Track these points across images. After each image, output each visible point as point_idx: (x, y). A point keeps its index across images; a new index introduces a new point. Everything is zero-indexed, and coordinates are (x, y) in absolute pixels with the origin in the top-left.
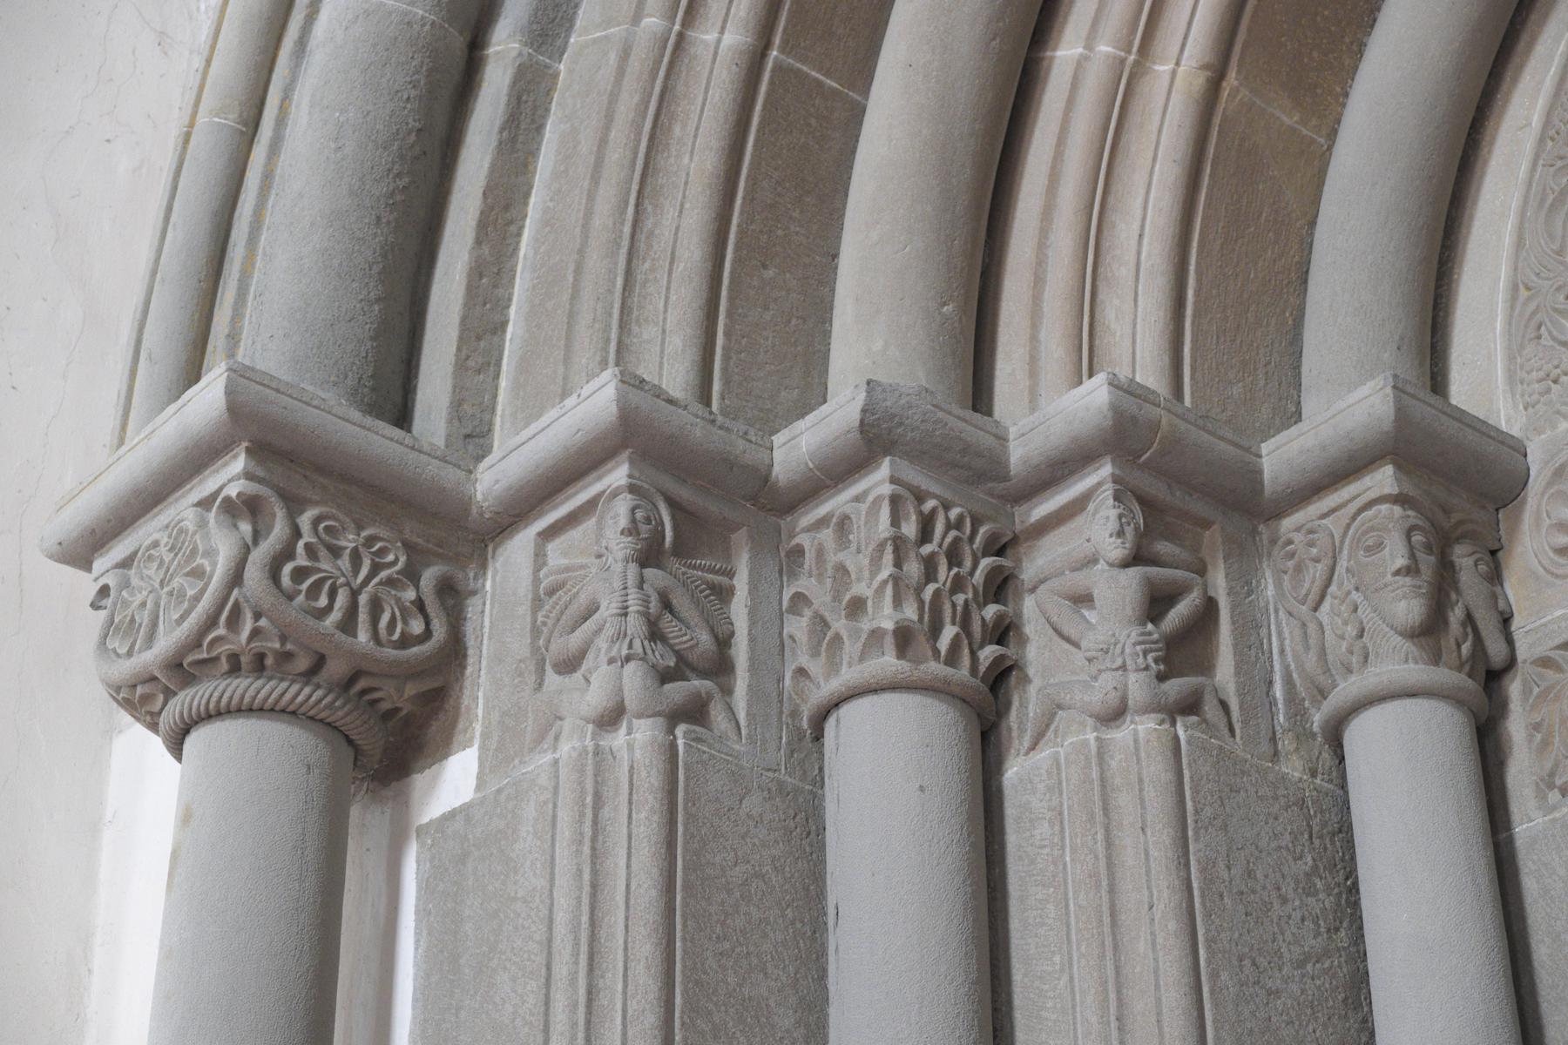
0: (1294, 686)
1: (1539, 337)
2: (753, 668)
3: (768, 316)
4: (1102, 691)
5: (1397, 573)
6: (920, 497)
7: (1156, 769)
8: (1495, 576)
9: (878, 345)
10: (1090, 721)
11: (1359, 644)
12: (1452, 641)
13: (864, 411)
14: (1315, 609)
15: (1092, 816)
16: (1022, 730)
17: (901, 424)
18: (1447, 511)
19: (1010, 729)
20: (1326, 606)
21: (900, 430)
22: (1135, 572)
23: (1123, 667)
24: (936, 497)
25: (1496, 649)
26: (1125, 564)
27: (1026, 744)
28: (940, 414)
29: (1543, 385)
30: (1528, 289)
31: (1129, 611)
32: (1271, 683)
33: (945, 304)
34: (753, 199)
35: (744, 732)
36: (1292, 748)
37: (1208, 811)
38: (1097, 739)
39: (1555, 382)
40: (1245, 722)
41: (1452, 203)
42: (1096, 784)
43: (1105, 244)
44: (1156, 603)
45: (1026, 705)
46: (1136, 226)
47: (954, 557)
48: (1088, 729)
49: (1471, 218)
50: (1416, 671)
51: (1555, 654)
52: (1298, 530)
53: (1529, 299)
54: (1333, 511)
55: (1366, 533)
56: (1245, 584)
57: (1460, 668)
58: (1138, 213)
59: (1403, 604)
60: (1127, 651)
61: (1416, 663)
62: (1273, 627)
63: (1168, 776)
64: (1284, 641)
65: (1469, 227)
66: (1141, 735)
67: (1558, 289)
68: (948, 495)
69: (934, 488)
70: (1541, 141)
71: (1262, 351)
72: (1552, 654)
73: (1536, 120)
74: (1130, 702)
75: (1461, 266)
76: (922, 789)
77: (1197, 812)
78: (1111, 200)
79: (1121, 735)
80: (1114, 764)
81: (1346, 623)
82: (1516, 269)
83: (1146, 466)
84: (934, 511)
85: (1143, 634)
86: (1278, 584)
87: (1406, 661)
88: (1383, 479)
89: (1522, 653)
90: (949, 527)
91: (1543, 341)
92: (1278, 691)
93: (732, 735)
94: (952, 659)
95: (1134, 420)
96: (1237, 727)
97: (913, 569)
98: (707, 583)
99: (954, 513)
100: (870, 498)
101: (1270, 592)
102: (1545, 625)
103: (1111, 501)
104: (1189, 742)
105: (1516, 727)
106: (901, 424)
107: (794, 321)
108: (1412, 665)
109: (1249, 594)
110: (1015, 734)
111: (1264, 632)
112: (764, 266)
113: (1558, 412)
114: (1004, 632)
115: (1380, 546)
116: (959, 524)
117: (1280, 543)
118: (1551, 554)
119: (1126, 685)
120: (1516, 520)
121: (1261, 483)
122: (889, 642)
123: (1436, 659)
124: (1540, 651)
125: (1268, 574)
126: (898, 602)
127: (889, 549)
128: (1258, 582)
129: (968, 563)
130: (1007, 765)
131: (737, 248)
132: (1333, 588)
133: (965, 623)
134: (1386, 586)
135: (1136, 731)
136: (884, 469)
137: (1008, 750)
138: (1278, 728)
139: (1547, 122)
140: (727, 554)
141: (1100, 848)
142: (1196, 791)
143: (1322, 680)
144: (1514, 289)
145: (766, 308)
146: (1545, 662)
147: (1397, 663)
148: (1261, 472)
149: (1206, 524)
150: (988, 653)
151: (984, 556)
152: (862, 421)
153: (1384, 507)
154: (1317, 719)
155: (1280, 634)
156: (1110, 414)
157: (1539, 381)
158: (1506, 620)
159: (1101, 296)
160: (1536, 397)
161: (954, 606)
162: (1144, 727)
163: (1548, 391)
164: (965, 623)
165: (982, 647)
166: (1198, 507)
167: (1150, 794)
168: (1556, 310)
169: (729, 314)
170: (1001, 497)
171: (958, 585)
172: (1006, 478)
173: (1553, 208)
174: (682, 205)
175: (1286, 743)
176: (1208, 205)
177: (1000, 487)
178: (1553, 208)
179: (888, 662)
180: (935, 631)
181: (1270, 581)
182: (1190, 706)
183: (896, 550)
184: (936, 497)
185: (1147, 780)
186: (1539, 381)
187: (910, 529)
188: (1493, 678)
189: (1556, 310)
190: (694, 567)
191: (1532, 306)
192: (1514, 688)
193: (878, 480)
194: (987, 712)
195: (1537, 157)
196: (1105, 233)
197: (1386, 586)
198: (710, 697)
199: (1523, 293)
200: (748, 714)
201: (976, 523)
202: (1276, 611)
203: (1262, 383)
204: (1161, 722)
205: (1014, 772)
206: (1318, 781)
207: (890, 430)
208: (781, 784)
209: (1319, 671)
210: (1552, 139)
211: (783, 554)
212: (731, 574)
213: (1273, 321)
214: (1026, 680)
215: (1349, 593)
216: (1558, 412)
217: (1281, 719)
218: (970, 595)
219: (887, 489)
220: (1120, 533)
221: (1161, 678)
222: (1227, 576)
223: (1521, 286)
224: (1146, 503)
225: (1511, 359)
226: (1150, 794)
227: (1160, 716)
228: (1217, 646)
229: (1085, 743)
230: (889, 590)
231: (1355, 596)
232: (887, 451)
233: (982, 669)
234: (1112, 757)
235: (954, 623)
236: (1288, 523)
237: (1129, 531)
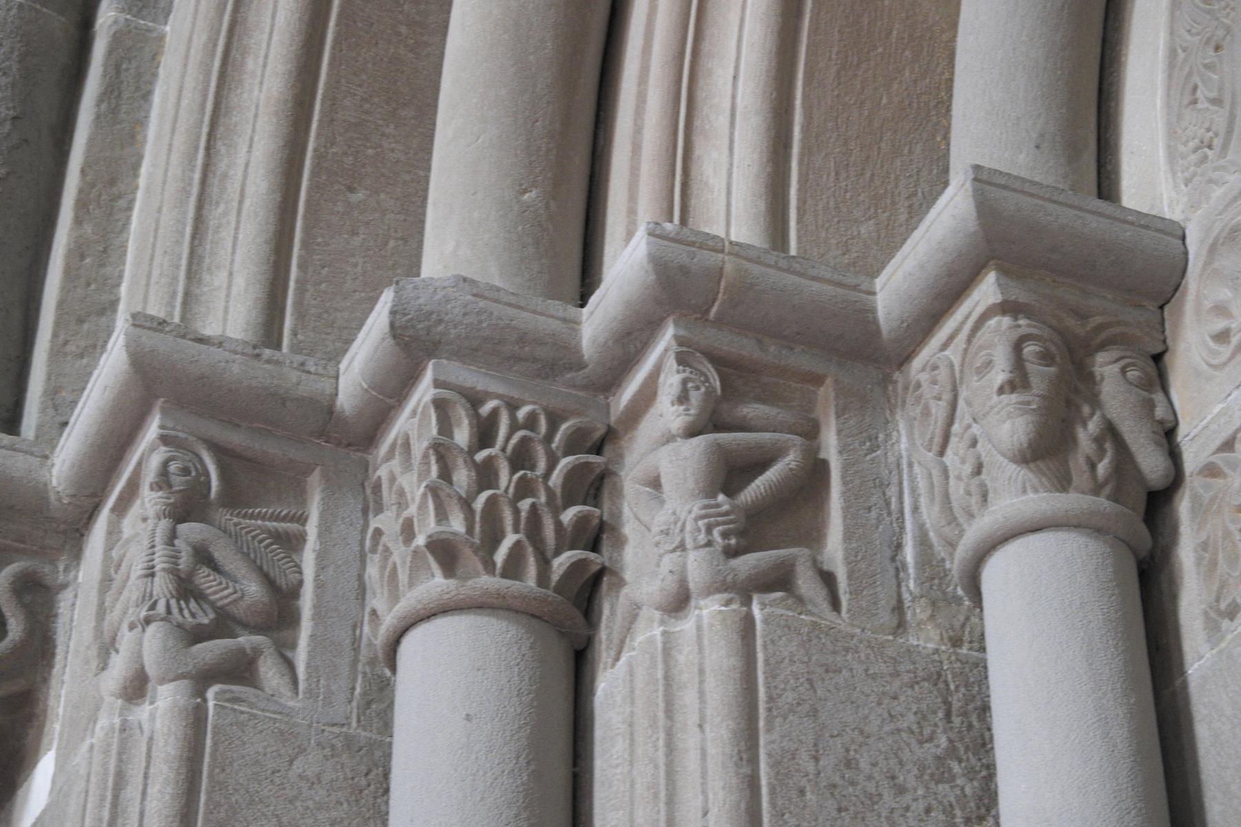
0: (931, 547)
1: (1195, 102)
2: (318, 615)
3: (357, 241)
5: (1001, 391)
6: (474, 400)
7: (720, 656)
9: (450, 246)
11: (976, 481)
12: (1082, 460)
13: (393, 313)
14: (942, 453)
15: (654, 719)
17: (441, 321)
18: (1082, 316)
21: (440, 328)
22: (700, 441)
23: (682, 547)
24: (498, 396)
25: (1151, 464)
26: (692, 432)
28: (482, 304)
31: (691, 484)
32: (899, 546)
33: (525, 191)
34: (332, 120)
35: (302, 686)
36: (924, 616)
37: (790, 696)
38: (664, 633)
40: (855, 593)
43: (701, 95)
44: (730, 473)
46: (731, 71)
47: (521, 458)
48: (656, 625)
52: (923, 369)
53: (1185, 60)
54: (951, 338)
56: (868, 439)
57: (1096, 490)
59: (1007, 426)
60: (688, 528)
61: (1036, 491)
62: (905, 484)
66: (706, 621)
68: (515, 394)
71: (903, 182)
72: (1212, 459)
74: (691, 586)
75: (1127, 47)
76: (468, 718)
77: (771, 699)
78: (706, 47)
79: (686, 626)
80: (682, 659)
81: (963, 462)
83: (719, 322)
84: (495, 413)
85: (706, 507)
87: (1024, 492)
88: (987, 291)
90: (514, 427)
91: (1200, 106)
92: (909, 554)
93: (286, 691)
94: (513, 568)
95: (684, 270)
96: (844, 599)
97: (463, 477)
98: (269, 532)
99: (522, 413)
100: (420, 410)
102: (1206, 427)
103: (675, 366)
104: (766, 621)
106: (441, 321)
107: (392, 243)
108: (1031, 495)
109: (872, 450)
110: (604, 646)
111: (892, 491)
112: (351, 189)
114: (596, 535)
116: (531, 422)
117: (911, 388)
119: (684, 566)
120: (1179, 313)
123: (1063, 482)
126: (442, 515)
128: (888, 436)
129: (542, 465)
131: (314, 174)
132: (956, 428)
133: (534, 526)
134: (992, 408)
135: (700, 618)
138: (906, 596)
140: (301, 496)
141: (661, 754)
142: (771, 675)
145: (354, 233)
146: (1211, 471)
147: (1016, 494)
148: (873, 311)
149: (818, 380)
151: (566, 454)
152: (392, 325)
155: (914, 490)
156: (650, 268)
157: (1195, 151)
159: (698, 151)
161: (517, 512)
162: (710, 610)
164: (534, 526)
165: (557, 553)
166: (802, 360)
167: (711, 683)
169: (305, 244)
170: (585, 388)
171: (524, 489)
172: (581, 365)
174: (252, 139)
175: (917, 612)
176: (814, 31)
179: (436, 584)
180: (493, 539)
181: (903, 432)
182: (778, 581)
183: (441, 459)
184: (498, 396)
185: (708, 670)
186: (1195, 151)
187: (462, 435)
190: (252, 517)
192: (1184, 507)
194: (569, 628)
196: (701, 83)
197: (992, 408)
198: (257, 652)
200: (308, 666)
201: (554, 421)
202: (910, 465)
203: (903, 217)
204: (727, 603)
206: (964, 651)
207: (428, 330)
208: (349, 742)
209: (943, 522)
211: (368, 491)
212: (302, 520)
213: (918, 149)
214: (621, 583)
215: (969, 427)
216: (1210, 181)
217: (912, 585)
218: (543, 499)
221: (731, 553)
222: (839, 432)
223: (1180, 51)
224: (718, 361)
226: (711, 683)
227: (726, 596)
228: (829, 514)
233: (555, 577)
234: (680, 652)
235: (516, 531)
236: (917, 363)
237: (696, 397)
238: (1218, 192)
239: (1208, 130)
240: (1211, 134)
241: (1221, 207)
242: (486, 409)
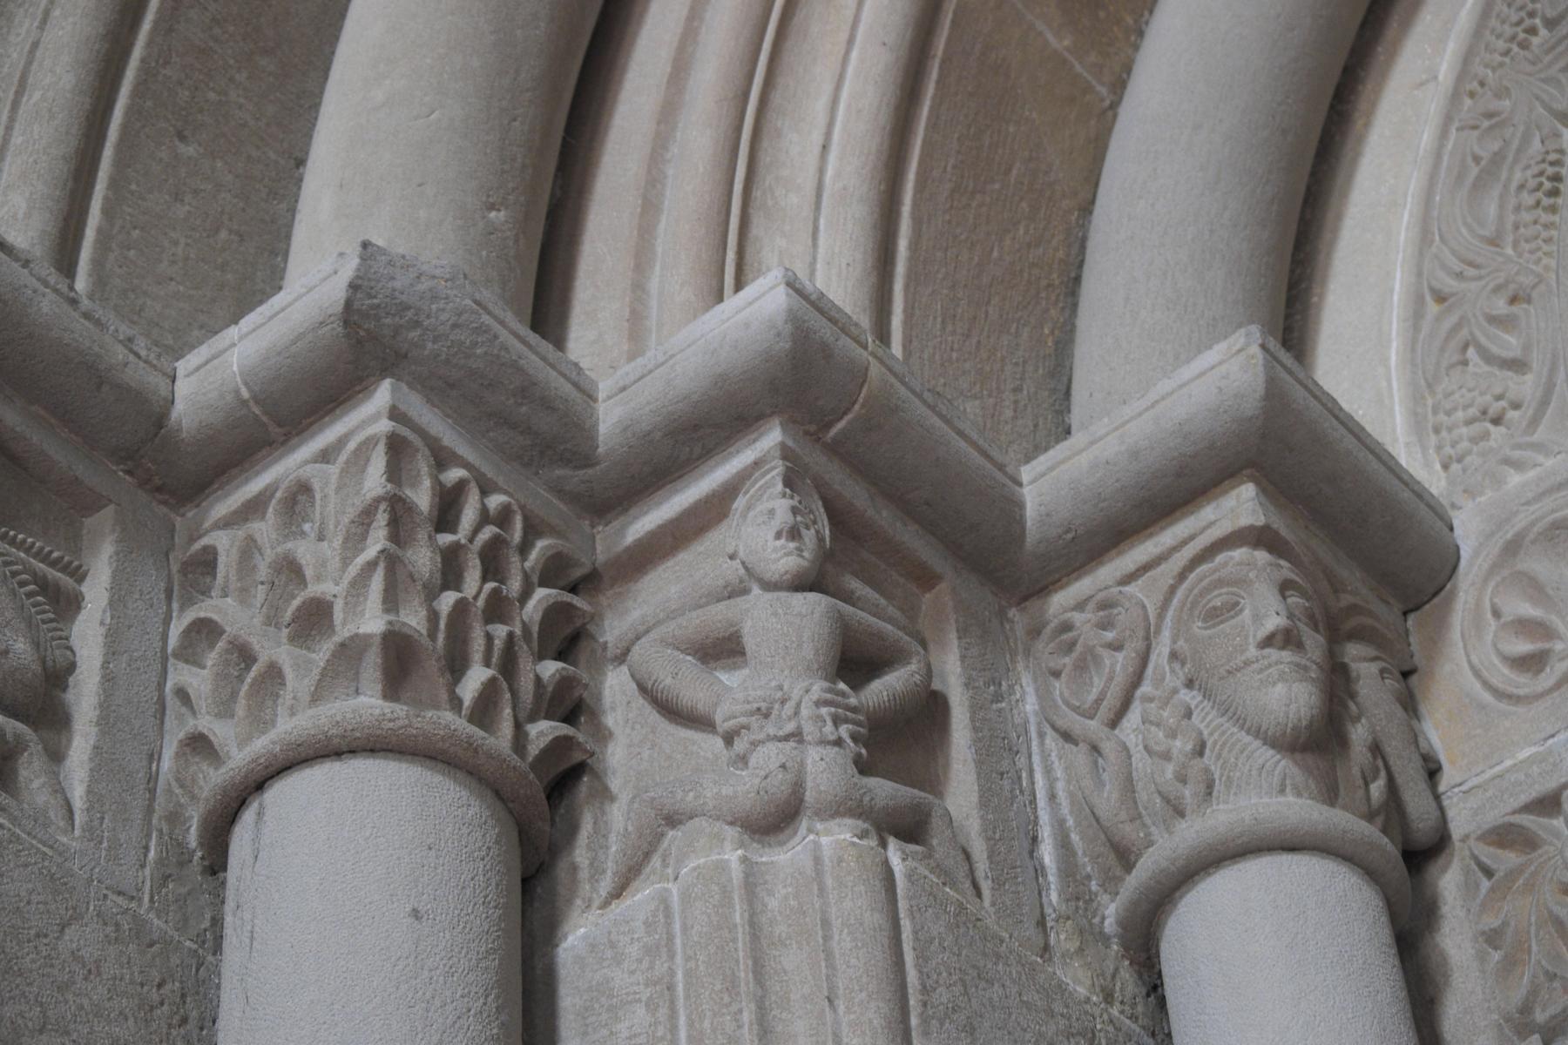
0: (1074, 854)
1: (1465, 363)
2: (107, 719)
3: (181, 211)
4: (759, 774)
5: (1268, 642)
6: (442, 459)
7: (854, 905)
8: (1410, 704)
10: (732, 833)
11: (1197, 764)
12: (1356, 771)
13: (354, 287)
14: (1114, 723)
16: (597, 871)
17: (417, 324)
19: (574, 869)
20: (1133, 717)
21: (414, 335)
23: (797, 736)
24: (466, 465)
27: (606, 885)
28: (486, 319)
29: (1476, 428)
30: (1440, 298)
31: (808, 652)
32: (1035, 840)
33: (492, 207)
34: (171, 30)
35: (79, 818)
36: (1073, 946)
37: (942, 996)
38: (744, 860)
39: (1497, 421)
40: (998, 884)
41: (1306, 201)
42: (741, 935)
43: (764, 159)
44: (854, 661)
45: (605, 830)
46: (817, 137)
47: (492, 565)
48: (728, 845)
49: (1339, 217)
50: (1299, 808)
51: (1526, 820)
52: (1080, 606)
54: (1145, 568)
55: (1208, 590)
56: (991, 685)
57: (1370, 817)
58: (821, 119)
59: (1280, 688)
60: (805, 712)
61: (1299, 795)
62: (1036, 759)
63: (875, 919)
64: (1053, 778)
65: (1336, 231)
66: (827, 853)
67: (1497, 289)
68: (489, 471)
69: (464, 450)
70: (1455, 96)
71: (1008, 368)
72: (1517, 819)
73: (1446, 68)
74: (809, 796)
75: (1324, 283)
76: (416, 914)
77: (924, 989)
78: (776, 98)
79: (787, 857)
80: (773, 903)
81: (1173, 735)
82: (1419, 274)
83: (835, 449)
84: (461, 486)
85: (830, 691)
86: (1044, 696)
87: (1282, 791)
88: (1241, 505)
89: (1461, 821)
90: (485, 518)
91: (1471, 368)
92: (1047, 854)
93: (56, 816)
94: (484, 711)
95: (826, 351)
96: (986, 887)
97: (422, 559)
98: (34, 574)
99: (495, 501)
100: (352, 445)
101: (1031, 705)
102: (1500, 776)
103: (780, 486)
104: (910, 876)
105: (1456, 940)
106: (417, 324)
107: (223, 234)
108: (1291, 799)
109: (998, 698)
110: (584, 874)
111: (1021, 761)
112: (182, 137)
113: (1507, 462)
115: (1233, 607)
116: (503, 518)
117: (1048, 630)
118: (1506, 671)
119: (802, 764)
120: (1441, 623)
121: (1021, 522)
122: (372, 668)
123: (1331, 795)
124: (1494, 816)
125: (1026, 680)
126: (391, 601)
127: (382, 518)
128: (1011, 687)
129: (515, 585)
130: (566, 928)
131: (137, 93)
132: (1146, 688)
133: (508, 666)
134: (1247, 663)
135: (817, 846)
136: (383, 394)
137: (570, 902)
138: (1048, 910)
139: (1462, 75)
140: (74, 541)
142: (922, 958)
143: (1129, 832)
144: (1419, 301)
145: (178, 197)
146: (1505, 836)
147: (1267, 793)
148: (1021, 506)
150: (543, 731)
151: (542, 584)
152: (348, 304)
153: (1239, 553)
154: (1111, 912)
155: (1048, 771)
156: (789, 328)
157: (1469, 422)
158: (1433, 772)
159: (756, 230)
160: (1465, 444)
161: (489, 638)
162: (834, 838)
163: (1486, 436)
164: (508, 666)
165: (533, 718)
167: (842, 941)
168: (1493, 320)
169: (114, 184)
170: (573, 498)
171: (497, 609)
172: (585, 459)
173: (1479, 186)
174: (47, 13)
175: (1062, 939)
176: (933, 125)
177: (575, 478)
178: (1479, 186)
179: (367, 704)
180: (456, 666)
181: (1030, 689)
182: (910, 827)
183: (394, 523)
184: (466, 465)
185: (836, 923)
186: (1469, 422)
187: (422, 498)
188: (1421, 854)
189: (1493, 320)
191: (1453, 319)
192: (1449, 881)
193: (371, 414)
195: (1448, 119)
196: (765, 143)
197: (1247, 663)
198: (19, 747)
199: (1433, 308)
200: (89, 791)
201: (533, 530)
202: (1041, 735)
203: (1009, 413)
204: (863, 835)
205: (578, 936)
206: (1115, 1011)
207: (397, 331)
208: (140, 926)
209: (1123, 815)
210: (1472, 95)
211: (175, 568)
212: (79, 575)
213: (1026, 332)
214: (604, 794)
215: (1175, 691)
217: (1054, 897)
218: (518, 631)
219: (384, 426)
220: (794, 533)
222: (963, 658)
223: (1428, 298)
225: (1416, 399)
227: (861, 824)
228: (947, 766)
229: (722, 867)
230: (377, 582)
231: (1186, 696)
232: (384, 373)
233: (533, 750)
234: (771, 893)
235: (487, 664)
236: (1060, 600)
237: (809, 536)
238: (1515, 479)
239: (1499, 398)
240: (1503, 403)
241: (1530, 495)
242: (454, 474)
